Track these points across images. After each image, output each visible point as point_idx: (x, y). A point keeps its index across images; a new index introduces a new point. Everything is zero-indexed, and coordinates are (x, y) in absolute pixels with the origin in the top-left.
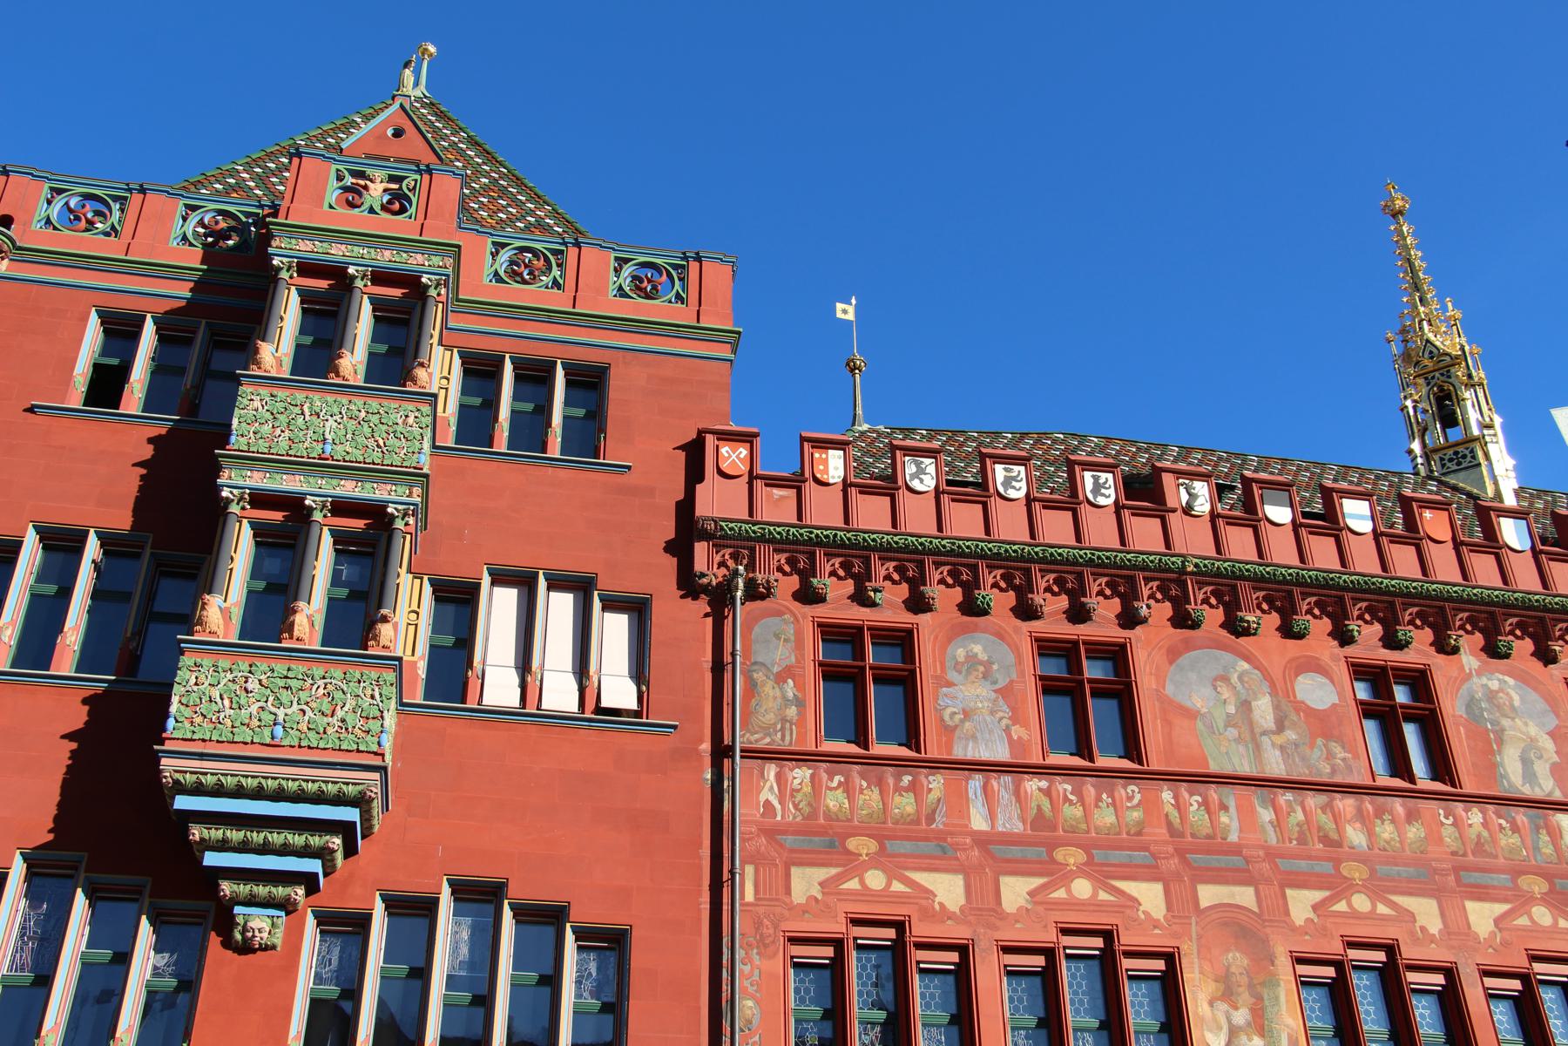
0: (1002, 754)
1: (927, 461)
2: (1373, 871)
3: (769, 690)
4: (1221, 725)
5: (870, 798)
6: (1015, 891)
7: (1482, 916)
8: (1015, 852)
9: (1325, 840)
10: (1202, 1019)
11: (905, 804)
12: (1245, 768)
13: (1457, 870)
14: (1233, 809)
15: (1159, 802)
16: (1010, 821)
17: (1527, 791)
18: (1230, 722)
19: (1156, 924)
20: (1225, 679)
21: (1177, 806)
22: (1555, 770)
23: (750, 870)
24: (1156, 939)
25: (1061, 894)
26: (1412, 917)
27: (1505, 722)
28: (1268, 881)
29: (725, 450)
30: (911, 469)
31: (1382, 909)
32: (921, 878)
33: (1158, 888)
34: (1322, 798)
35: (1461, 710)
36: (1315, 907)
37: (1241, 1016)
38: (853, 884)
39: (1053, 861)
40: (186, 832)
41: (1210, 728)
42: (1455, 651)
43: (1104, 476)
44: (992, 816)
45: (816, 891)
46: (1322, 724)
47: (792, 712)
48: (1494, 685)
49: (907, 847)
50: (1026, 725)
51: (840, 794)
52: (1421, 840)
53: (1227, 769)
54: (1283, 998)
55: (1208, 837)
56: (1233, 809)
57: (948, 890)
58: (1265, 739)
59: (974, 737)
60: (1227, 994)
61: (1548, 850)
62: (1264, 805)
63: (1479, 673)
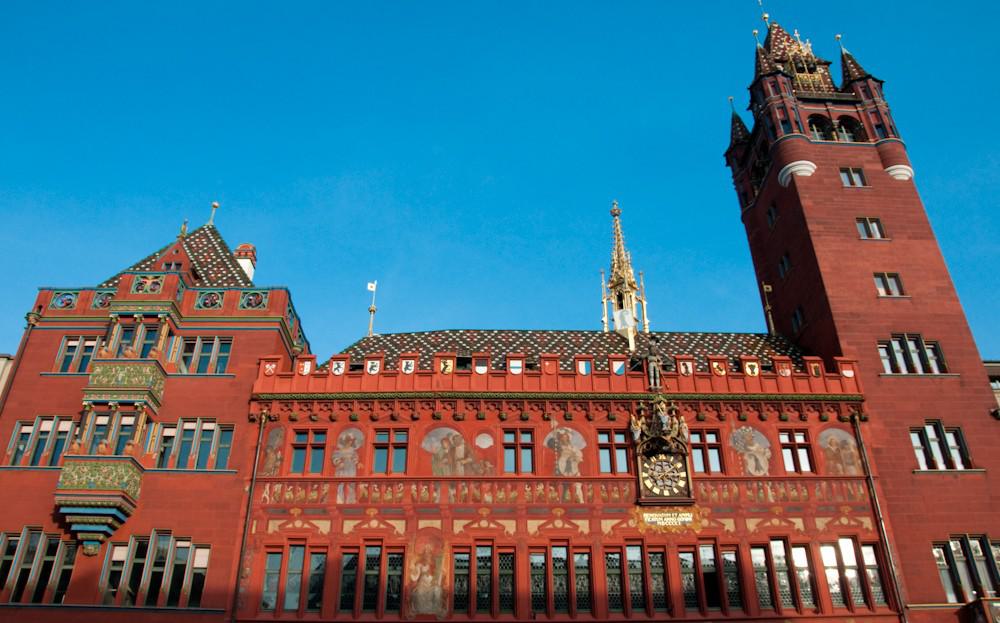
0: (352, 474)
1: (342, 363)
2: (491, 513)
3: (272, 456)
4: (441, 457)
5: (302, 493)
6: (349, 526)
8: (351, 511)
9: (476, 500)
10: (411, 571)
11: (314, 495)
12: (447, 473)
13: (527, 508)
14: (439, 491)
15: (410, 490)
16: (352, 500)
17: (566, 475)
18: (445, 456)
19: (399, 535)
21: (417, 491)
22: (581, 466)
23: (255, 522)
24: (399, 541)
25: (366, 526)
27: (563, 447)
28: (447, 518)
29: (267, 366)
30: (335, 366)
31: (492, 525)
32: (315, 522)
33: (404, 522)
34: (477, 484)
35: (545, 444)
36: (465, 527)
37: (426, 569)
38: (290, 526)
39: (365, 514)
40: (65, 519)
41: (437, 459)
43: (410, 361)
44: (345, 498)
45: (277, 529)
47: (279, 463)
48: (562, 432)
49: (310, 511)
50: (364, 464)
51: (291, 493)
52: (516, 498)
53: (440, 475)
54: (443, 560)
55: (428, 502)
56: (439, 491)
57: (324, 526)
58: (459, 463)
59: (343, 469)
61: (568, 497)
62: (452, 488)
63: (558, 427)
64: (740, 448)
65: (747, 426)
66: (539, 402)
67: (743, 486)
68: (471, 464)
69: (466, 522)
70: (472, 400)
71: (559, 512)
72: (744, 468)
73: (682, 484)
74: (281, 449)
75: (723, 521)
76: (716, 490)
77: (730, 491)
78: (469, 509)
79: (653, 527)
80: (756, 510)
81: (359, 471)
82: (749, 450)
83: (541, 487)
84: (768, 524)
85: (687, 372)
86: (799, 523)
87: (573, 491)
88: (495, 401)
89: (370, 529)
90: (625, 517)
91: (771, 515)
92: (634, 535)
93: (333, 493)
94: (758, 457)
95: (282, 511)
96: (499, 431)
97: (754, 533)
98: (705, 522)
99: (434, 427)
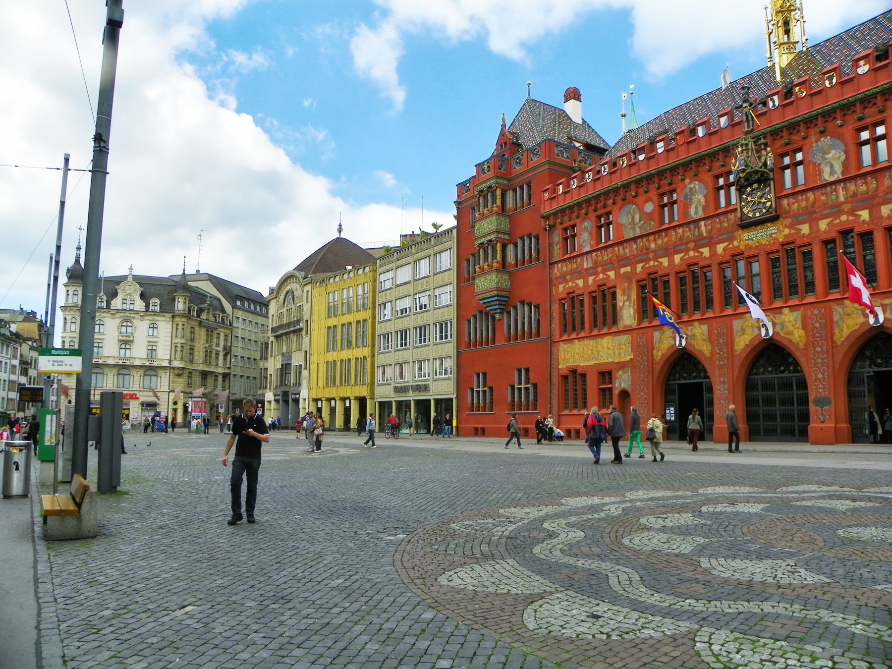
0: (588, 249)
6: (591, 279)
7: (677, 258)
9: (647, 249)
11: (574, 266)
12: (632, 236)
16: (590, 265)
17: (695, 217)
20: (629, 212)
26: (661, 263)
35: (682, 198)
36: (642, 268)
42: (683, 180)
46: (649, 216)
48: (692, 186)
57: (580, 283)
60: (624, 294)
61: (696, 234)
64: (817, 159)
65: (825, 136)
66: (673, 170)
67: (818, 193)
68: (643, 225)
69: (642, 265)
70: (638, 182)
71: (691, 245)
72: (820, 175)
73: (768, 204)
74: (558, 242)
75: (800, 227)
76: (797, 202)
77: (807, 200)
78: (644, 255)
79: (750, 242)
80: (829, 211)
81: (592, 246)
82: (826, 159)
83: (681, 230)
84: (838, 221)
85: (774, 105)
86: (865, 215)
87: (699, 227)
88: (649, 178)
89: (600, 280)
90: (731, 239)
91: (841, 212)
92: (736, 252)
93: (582, 262)
94: (833, 163)
95: (563, 278)
96: (655, 198)
97: (825, 232)
98: (787, 231)
99: (623, 205)
